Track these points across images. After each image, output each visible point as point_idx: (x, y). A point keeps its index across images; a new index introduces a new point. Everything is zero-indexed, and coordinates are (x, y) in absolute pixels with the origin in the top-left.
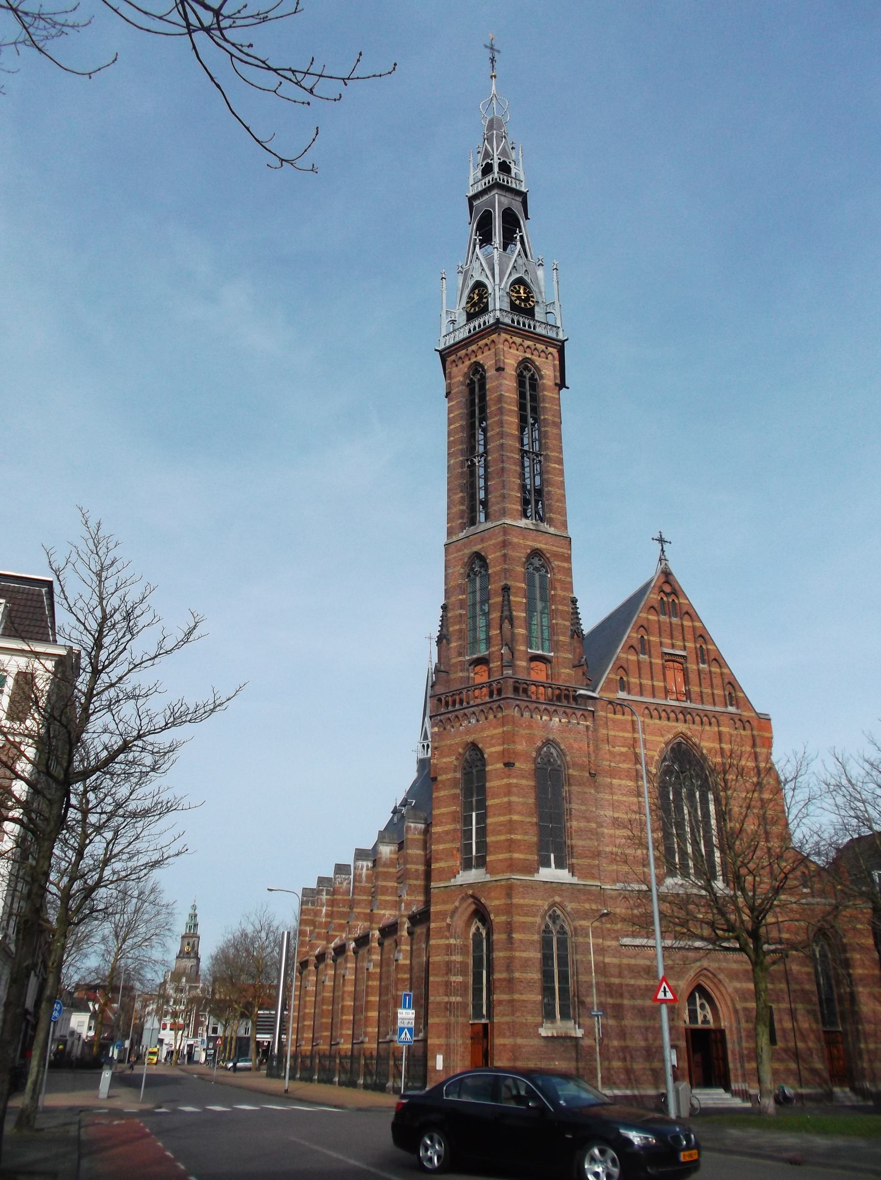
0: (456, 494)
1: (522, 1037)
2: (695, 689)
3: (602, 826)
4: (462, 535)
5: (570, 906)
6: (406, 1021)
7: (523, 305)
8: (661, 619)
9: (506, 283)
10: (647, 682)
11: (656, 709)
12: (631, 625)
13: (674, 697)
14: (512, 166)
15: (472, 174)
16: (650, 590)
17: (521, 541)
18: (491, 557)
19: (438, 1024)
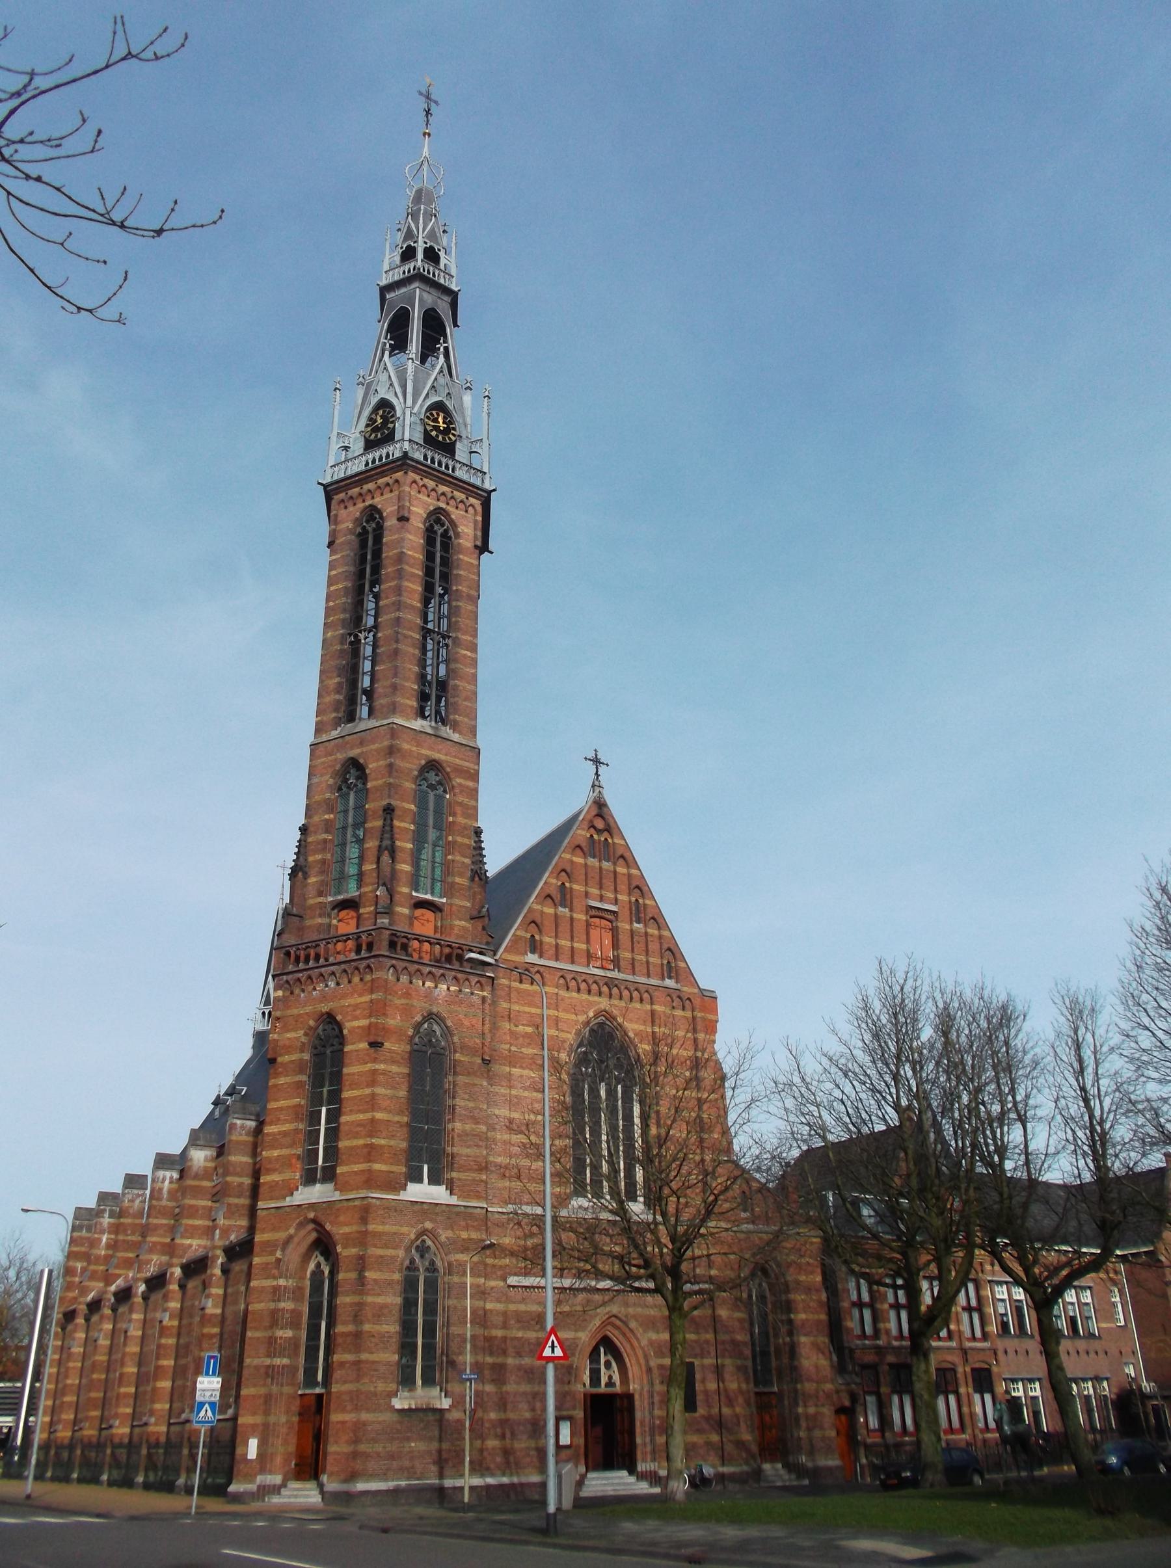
0: (331, 678)
1: (368, 1410)
2: (626, 955)
3: (494, 1129)
4: (334, 734)
5: (444, 1235)
6: (208, 1394)
7: (440, 438)
8: (589, 863)
9: (421, 406)
10: (565, 943)
11: (574, 978)
12: (550, 868)
13: (598, 964)
14: (442, 254)
15: (387, 257)
16: (578, 823)
17: (414, 749)
18: (371, 766)
19: (253, 1396)
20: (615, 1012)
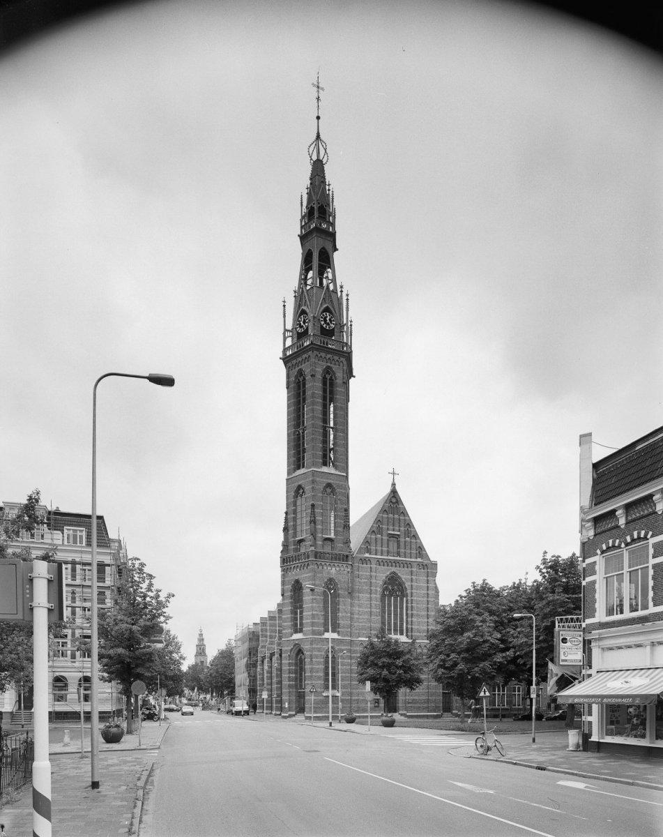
2: (402, 550)
20: (397, 572)
